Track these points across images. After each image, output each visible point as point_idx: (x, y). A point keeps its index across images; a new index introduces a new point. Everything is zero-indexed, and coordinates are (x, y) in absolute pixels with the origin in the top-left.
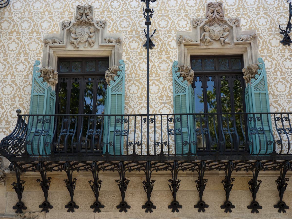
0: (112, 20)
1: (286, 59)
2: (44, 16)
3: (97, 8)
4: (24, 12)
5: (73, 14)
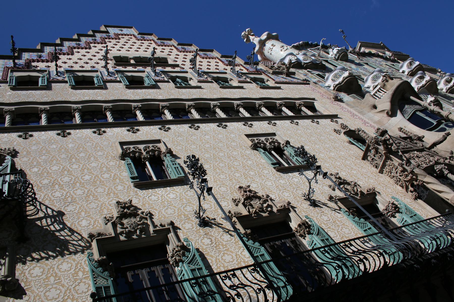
0: (156, 210)
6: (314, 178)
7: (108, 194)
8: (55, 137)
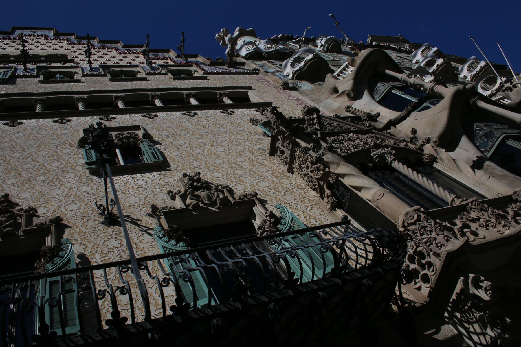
1: (110, 239)
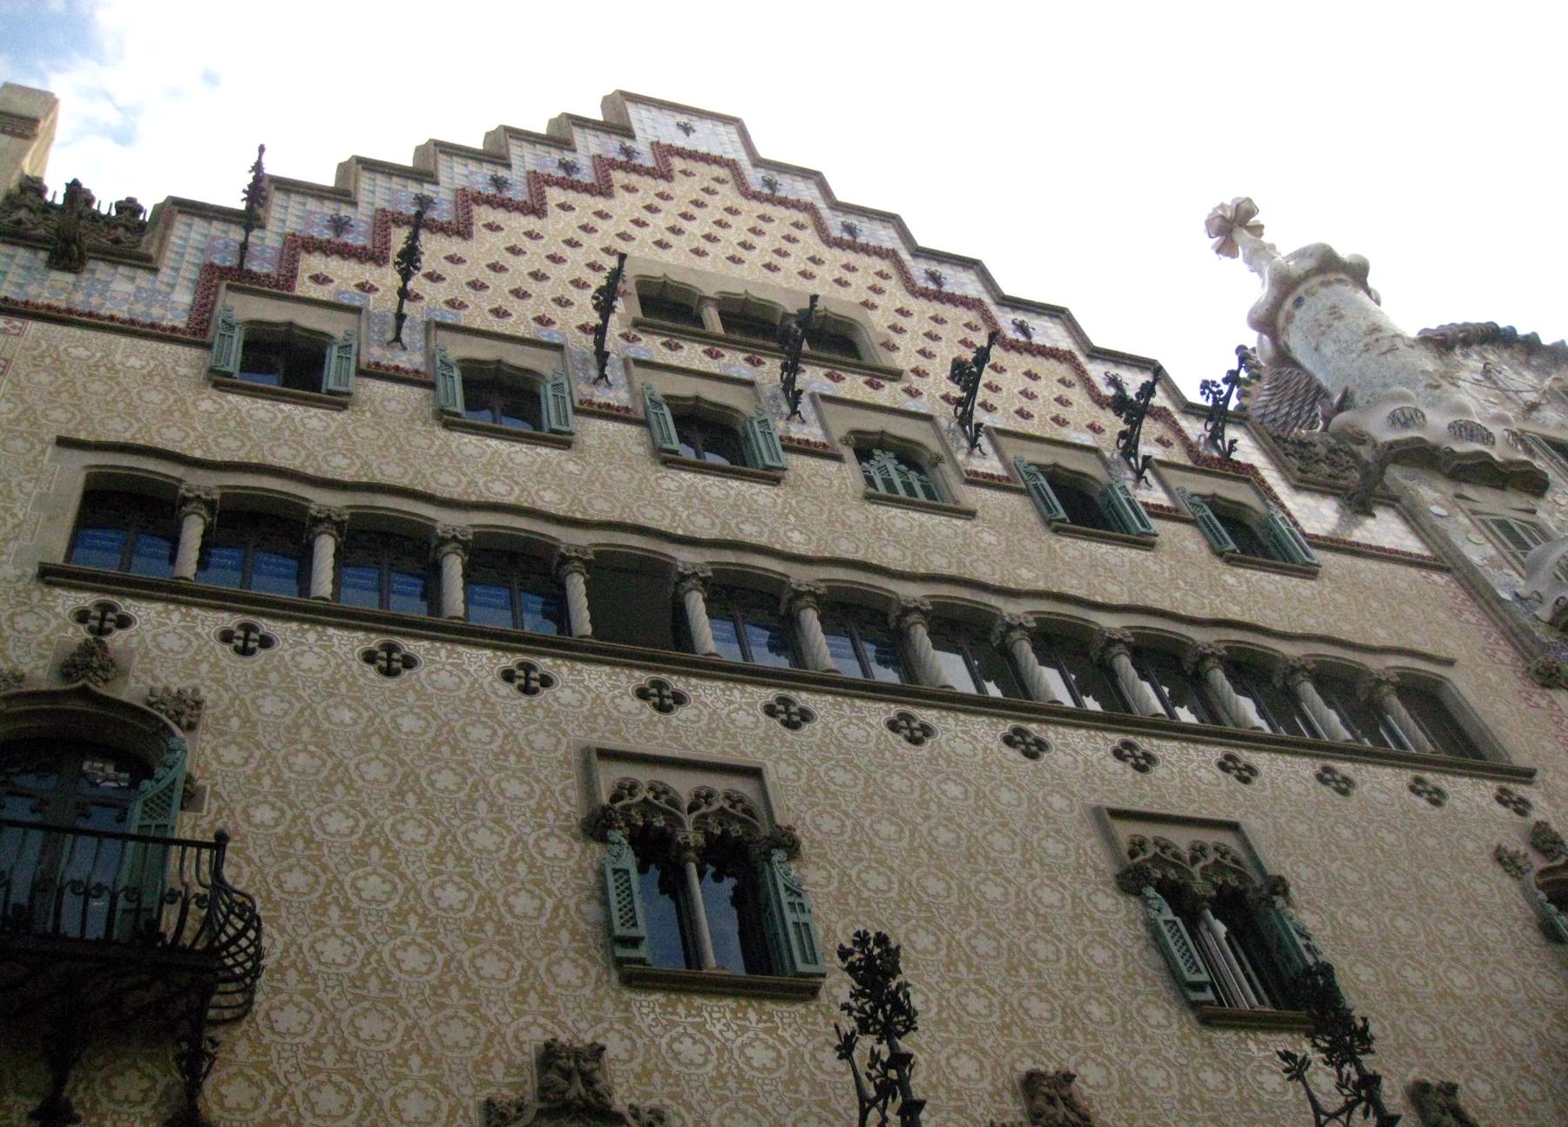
0: (689, 1107)
2: (405, 1070)
3: (617, 1058)
4: (319, 1048)
5: (526, 1073)
6: (1341, 1111)
7: (521, 994)
8: (355, 665)
